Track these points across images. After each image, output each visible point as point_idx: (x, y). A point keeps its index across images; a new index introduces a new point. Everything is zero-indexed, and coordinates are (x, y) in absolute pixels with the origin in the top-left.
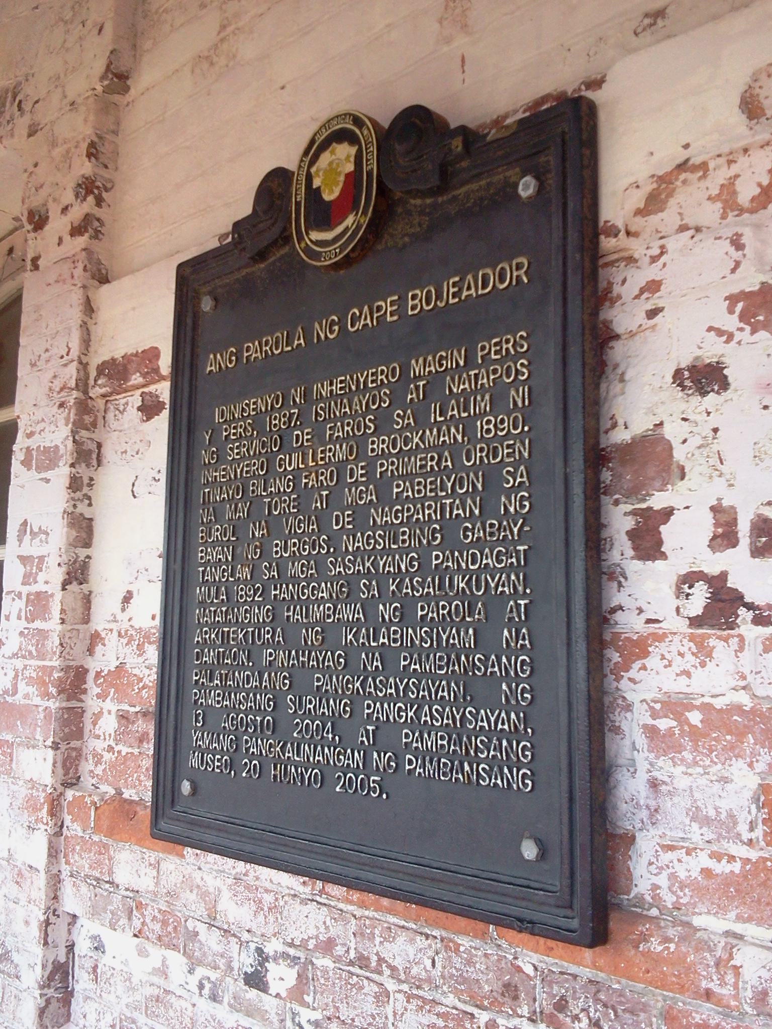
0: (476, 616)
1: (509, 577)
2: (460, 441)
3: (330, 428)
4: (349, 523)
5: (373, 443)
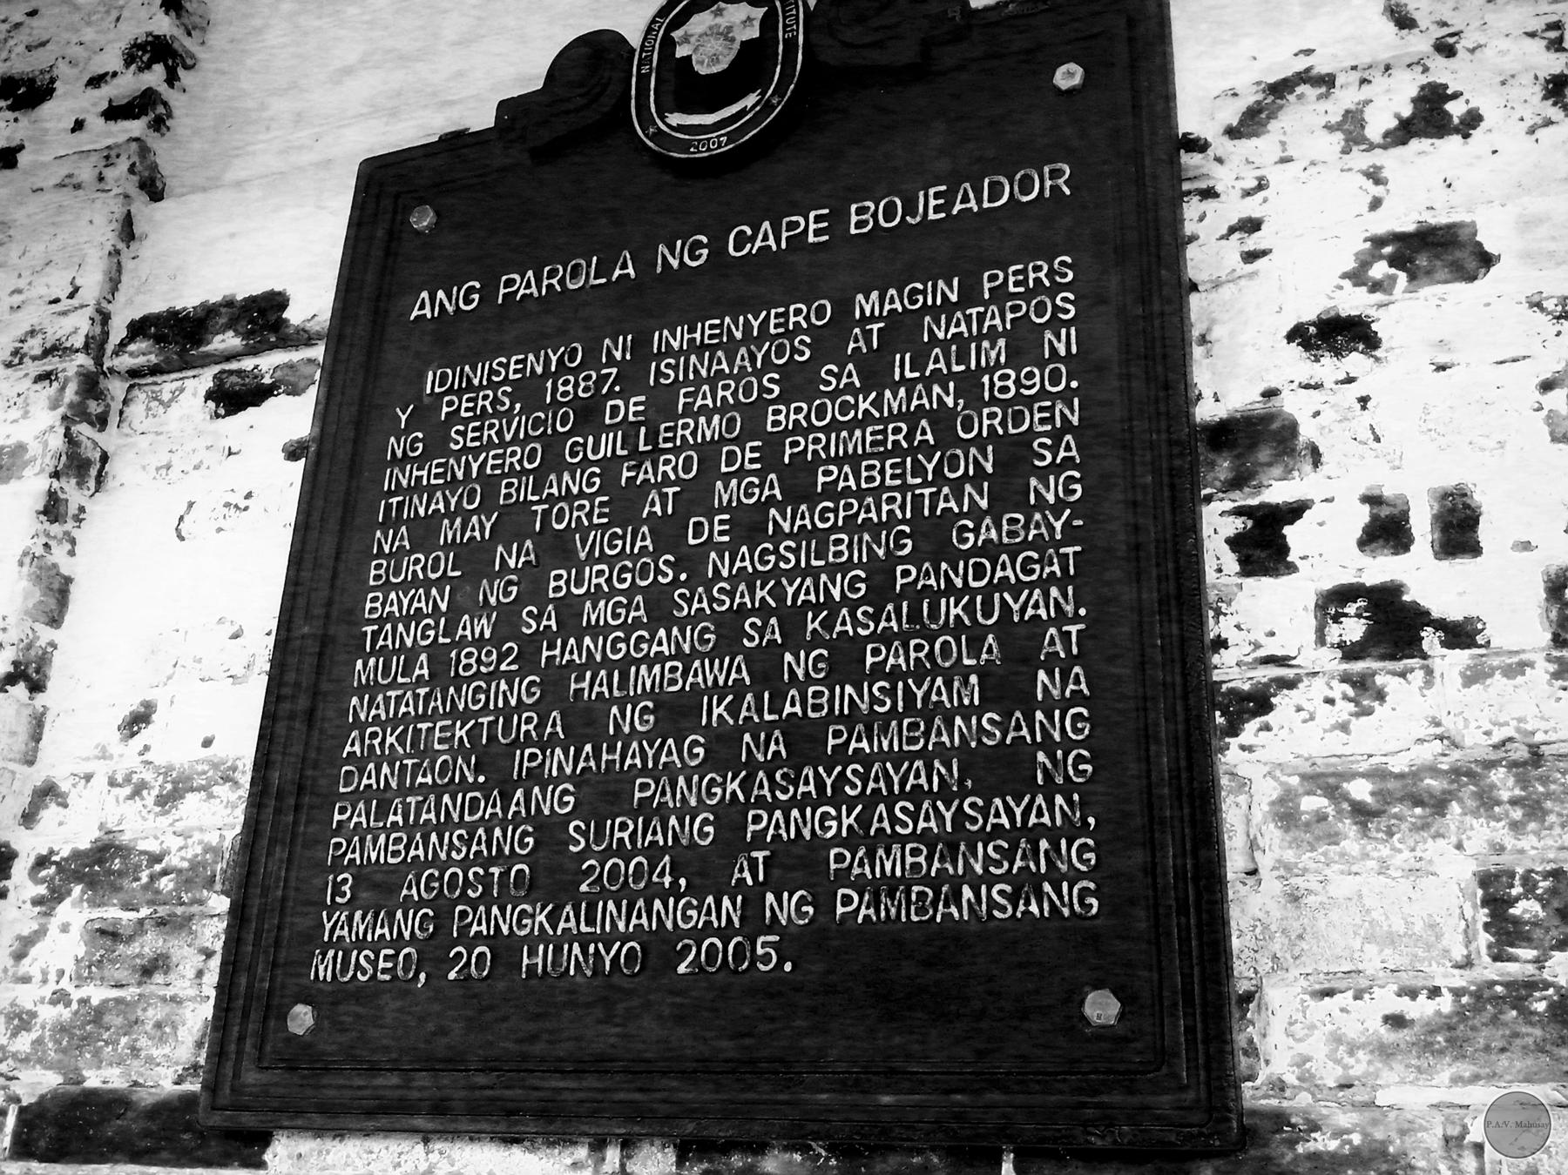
0: (984, 656)
1: (1046, 595)
2: (951, 405)
3: (686, 395)
4: (721, 533)
5: (777, 412)
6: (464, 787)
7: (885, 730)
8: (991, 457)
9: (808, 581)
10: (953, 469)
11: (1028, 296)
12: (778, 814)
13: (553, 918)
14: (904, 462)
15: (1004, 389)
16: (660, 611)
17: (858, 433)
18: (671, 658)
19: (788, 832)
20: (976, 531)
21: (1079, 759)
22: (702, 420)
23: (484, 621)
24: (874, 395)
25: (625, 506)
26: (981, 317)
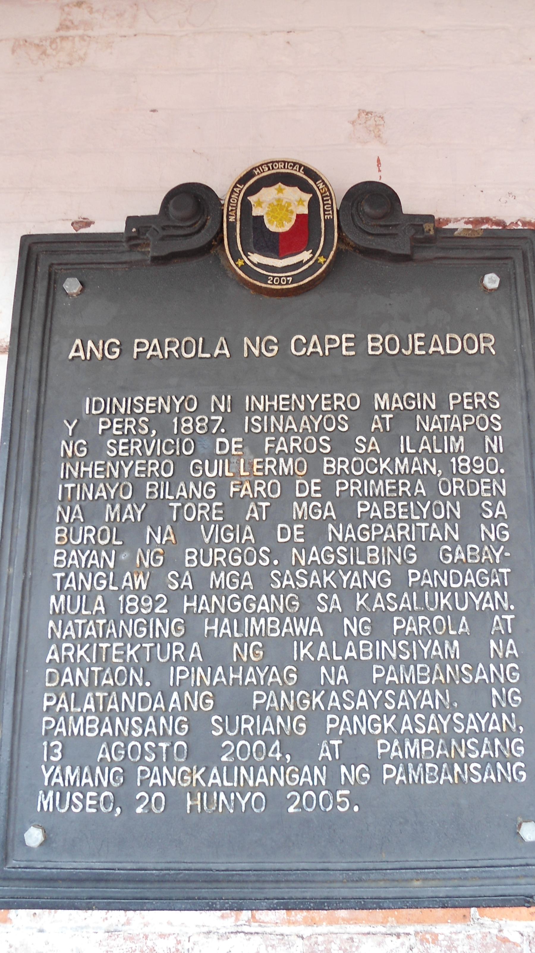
2: (434, 473)
3: (269, 442)
4: (298, 536)
6: (136, 688)
7: (407, 670)
8: (459, 509)
9: (356, 574)
10: (439, 513)
11: (475, 412)
12: (345, 718)
13: (205, 777)
14: (409, 504)
15: (464, 468)
16: (262, 583)
17: (381, 483)
18: (271, 614)
19: (352, 729)
20: (453, 553)
21: (515, 693)
22: (282, 460)
23: (141, 577)
24: (388, 460)
25: (233, 509)
26: (450, 420)
